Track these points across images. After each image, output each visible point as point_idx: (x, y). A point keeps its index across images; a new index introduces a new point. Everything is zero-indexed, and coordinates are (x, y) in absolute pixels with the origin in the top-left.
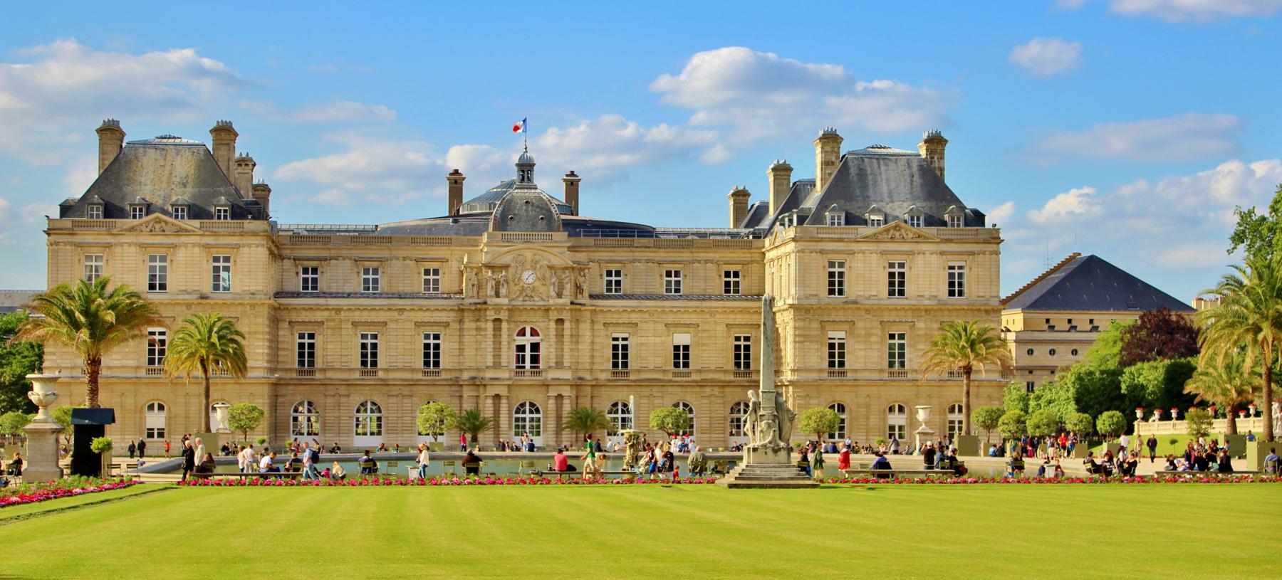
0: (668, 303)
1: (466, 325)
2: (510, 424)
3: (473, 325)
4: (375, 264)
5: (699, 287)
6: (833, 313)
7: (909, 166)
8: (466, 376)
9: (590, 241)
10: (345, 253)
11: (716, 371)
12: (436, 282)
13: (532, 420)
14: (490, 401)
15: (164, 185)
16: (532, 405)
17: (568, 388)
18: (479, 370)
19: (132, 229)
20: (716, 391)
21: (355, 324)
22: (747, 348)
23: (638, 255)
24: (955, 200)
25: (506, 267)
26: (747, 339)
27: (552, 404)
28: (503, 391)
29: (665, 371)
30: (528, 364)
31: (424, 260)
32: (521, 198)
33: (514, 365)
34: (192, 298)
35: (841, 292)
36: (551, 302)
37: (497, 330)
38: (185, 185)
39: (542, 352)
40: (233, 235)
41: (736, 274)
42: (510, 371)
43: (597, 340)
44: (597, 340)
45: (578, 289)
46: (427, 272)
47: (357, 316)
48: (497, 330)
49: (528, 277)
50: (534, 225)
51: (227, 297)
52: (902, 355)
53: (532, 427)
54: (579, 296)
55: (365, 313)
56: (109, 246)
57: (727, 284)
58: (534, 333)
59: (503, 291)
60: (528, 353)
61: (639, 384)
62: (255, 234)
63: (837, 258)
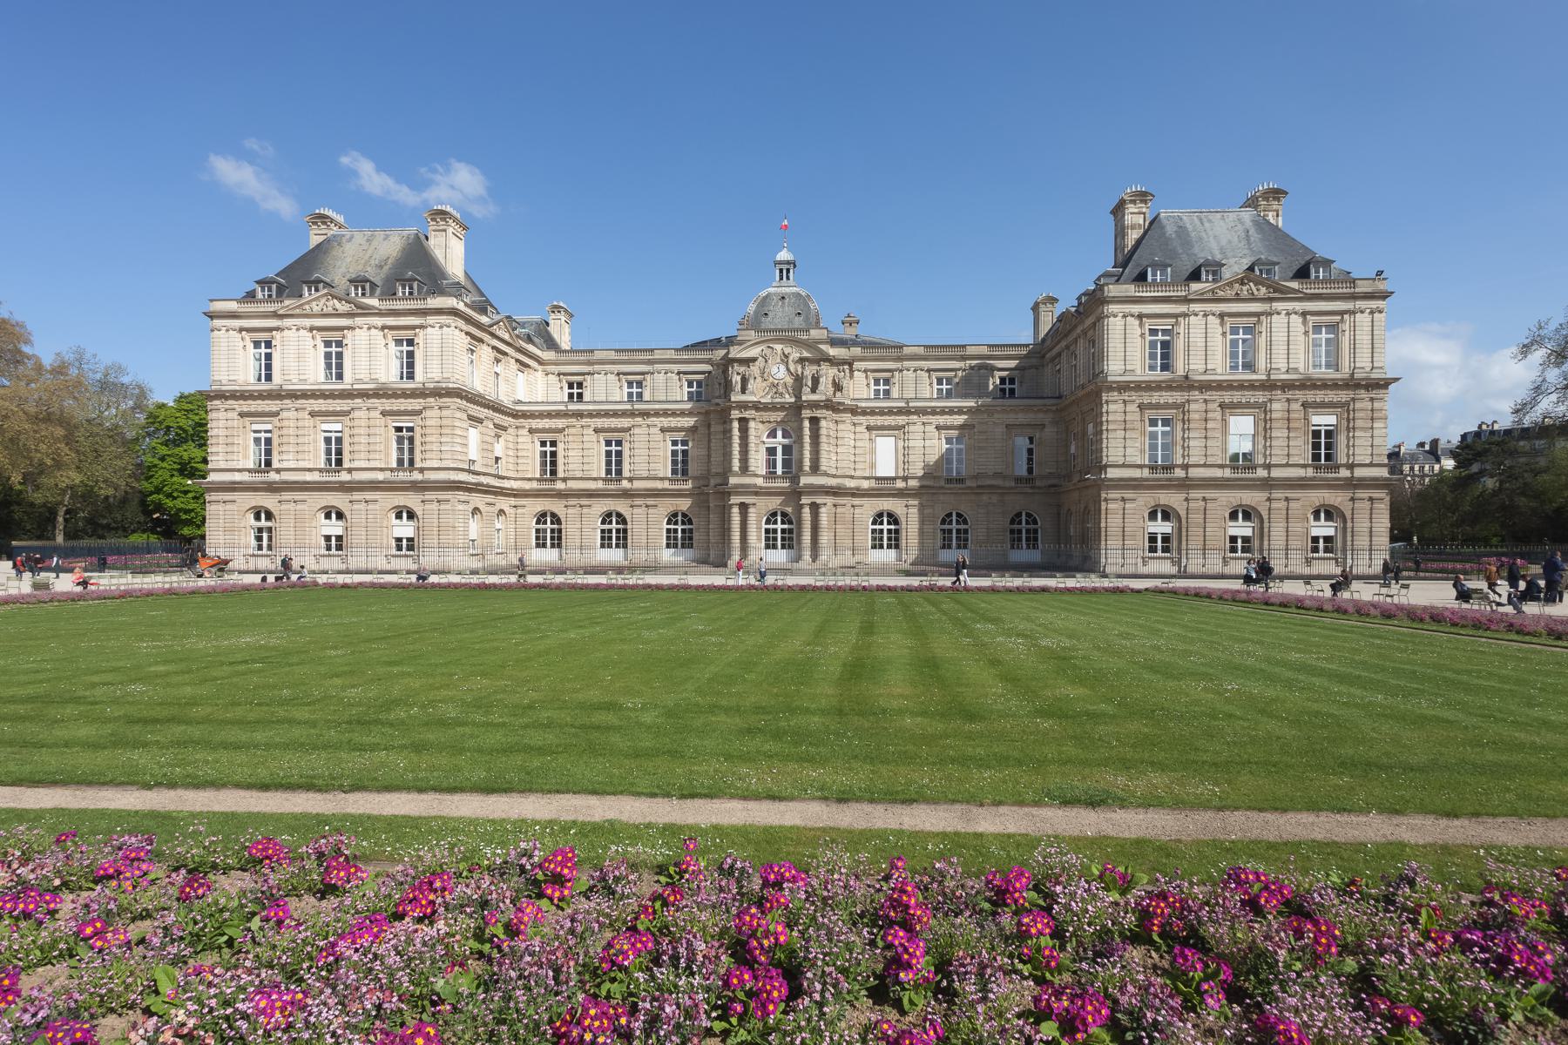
2: (759, 539)
3: (720, 428)
4: (639, 377)
8: (712, 482)
10: (608, 367)
11: (996, 475)
13: (783, 531)
14: (735, 510)
20: (995, 499)
21: (596, 431)
23: (906, 364)
25: (754, 360)
27: (806, 512)
30: (779, 470)
37: (744, 431)
38: (381, 267)
41: (1012, 381)
43: (859, 444)
44: (859, 444)
45: (838, 387)
49: (779, 373)
50: (790, 321)
51: (410, 385)
53: (783, 539)
54: (838, 394)
62: (439, 312)
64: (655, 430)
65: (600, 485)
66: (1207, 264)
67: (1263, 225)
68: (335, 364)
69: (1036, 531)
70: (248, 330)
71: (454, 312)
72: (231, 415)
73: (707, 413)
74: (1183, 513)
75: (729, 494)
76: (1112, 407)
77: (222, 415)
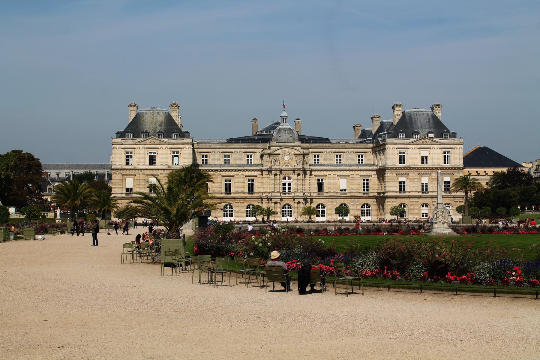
0: (338, 168)
1: (264, 176)
5: (349, 162)
7: (428, 114)
8: (264, 195)
9: (308, 145)
12: (251, 160)
13: (288, 211)
14: (273, 204)
15: (154, 125)
16: (289, 205)
18: (269, 193)
22: (367, 184)
24: (445, 128)
25: (279, 154)
26: (367, 180)
30: (287, 191)
31: (246, 152)
32: (283, 129)
33: (281, 191)
35: (404, 163)
36: (296, 167)
39: (292, 186)
41: (362, 156)
44: (312, 181)
46: (248, 157)
49: (286, 158)
50: (288, 139)
52: (426, 186)
53: (288, 214)
57: (359, 160)
58: (289, 178)
60: (287, 186)
61: (327, 198)
63: (402, 150)
65: (223, 195)
66: (416, 132)
67: (435, 118)
68: (152, 160)
69: (370, 210)
70: (125, 148)
72: (120, 175)
73: (262, 171)
74: (409, 206)
75: (271, 199)
76: (389, 175)
77: (117, 175)
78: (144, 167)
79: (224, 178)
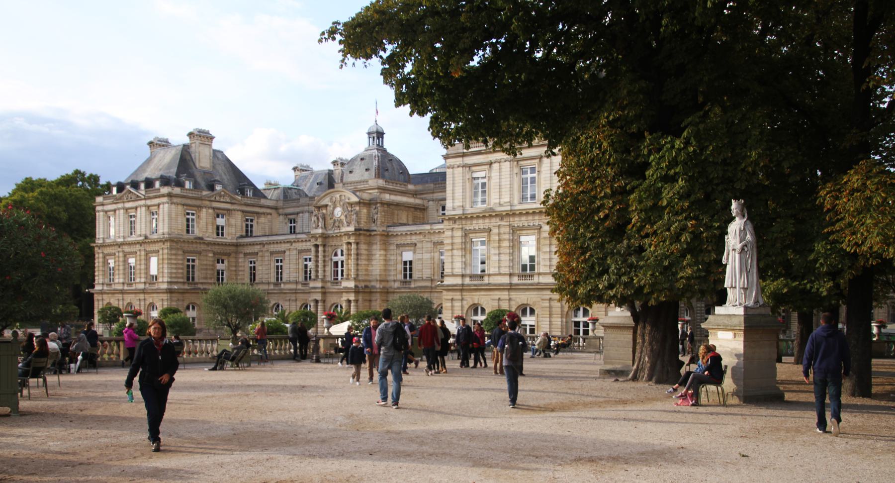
6: (474, 222)
10: (306, 208)
17: (353, 295)
19: (120, 198)
21: (272, 253)
25: (326, 206)
28: (319, 297)
29: (432, 280)
33: (329, 277)
34: (142, 238)
37: (317, 251)
40: (156, 197)
42: (323, 281)
43: (392, 258)
44: (392, 258)
47: (273, 248)
48: (317, 251)
49: (338, 212)
55: (276, 246)
56: (115, 211)
59: (320, 224)
62: (163, 196)
64: (295, 252)
71: (170, 195)
78: (121, 240)
79: (275, 258)
